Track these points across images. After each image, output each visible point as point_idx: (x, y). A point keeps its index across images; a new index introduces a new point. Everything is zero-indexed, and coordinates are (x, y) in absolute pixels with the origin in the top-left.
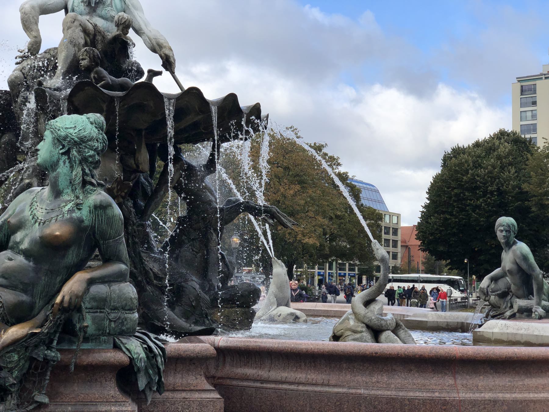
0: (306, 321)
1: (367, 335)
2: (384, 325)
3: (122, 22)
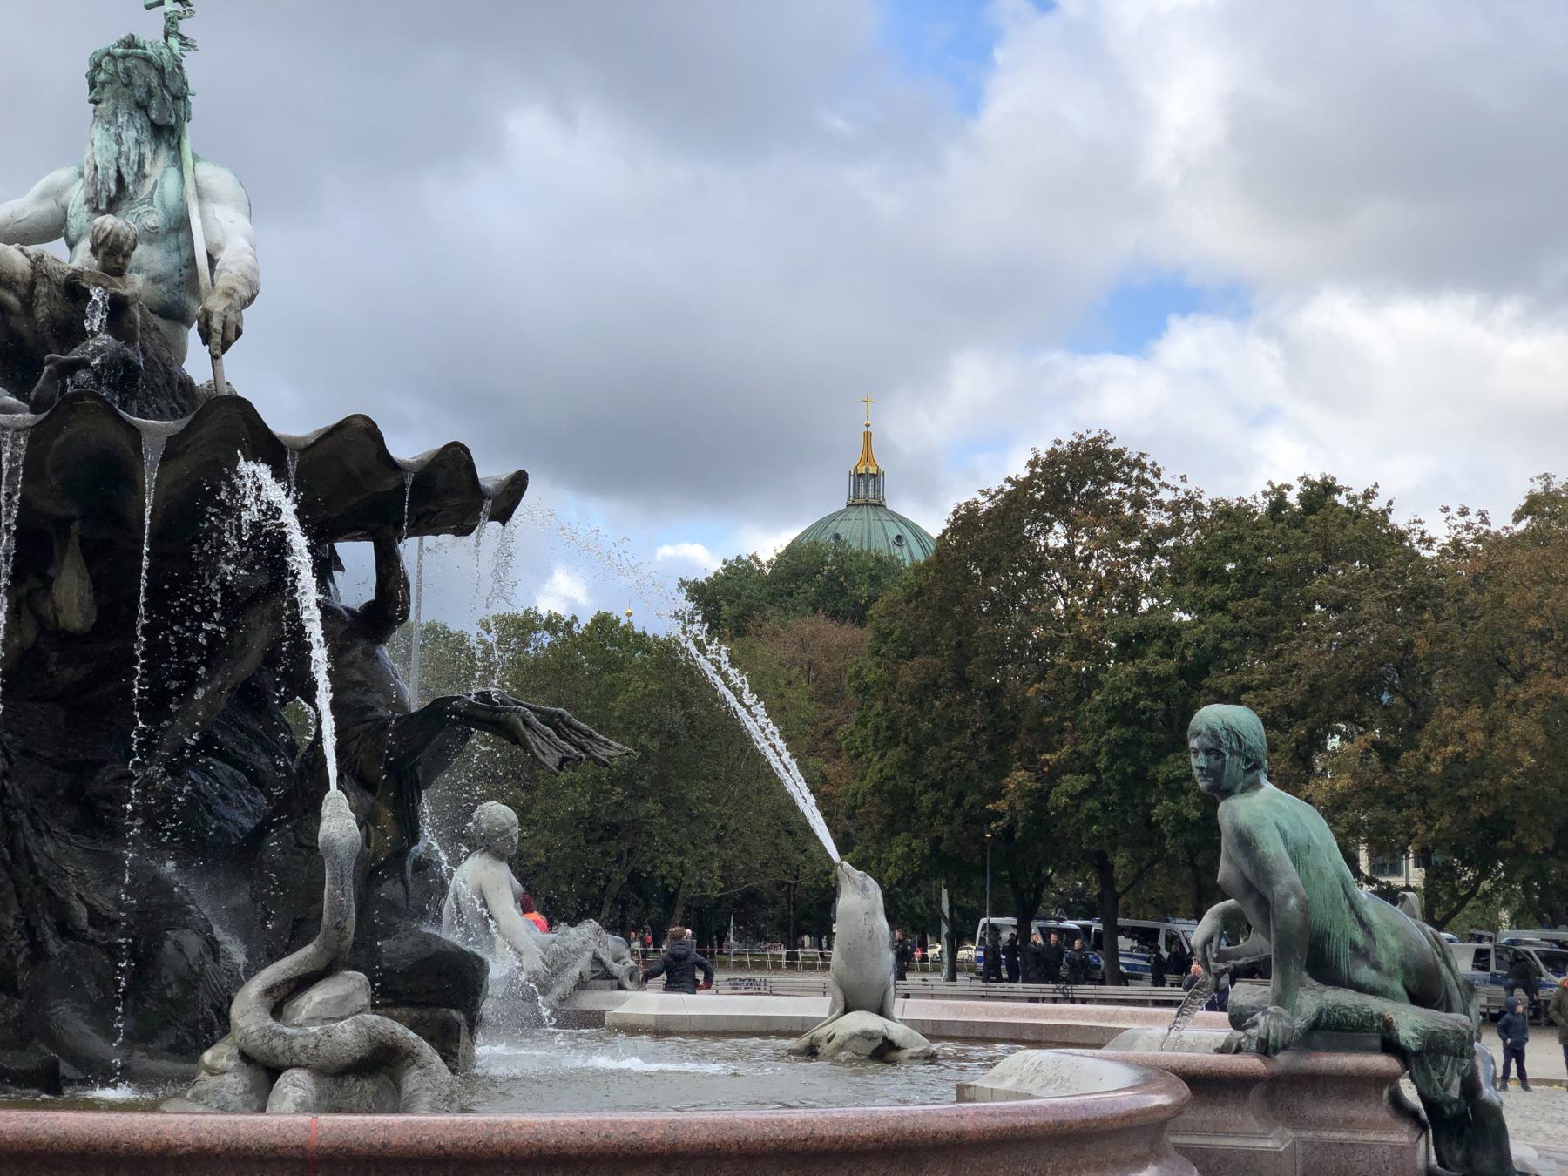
0: (931, 1058)
2: (280, 1049)
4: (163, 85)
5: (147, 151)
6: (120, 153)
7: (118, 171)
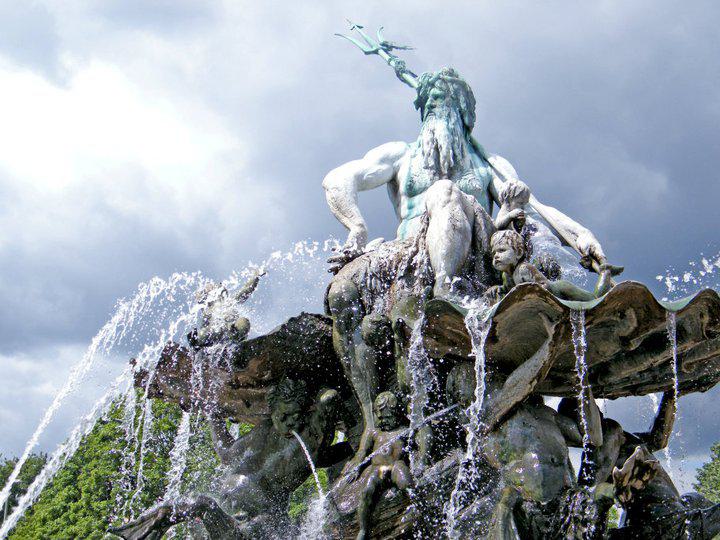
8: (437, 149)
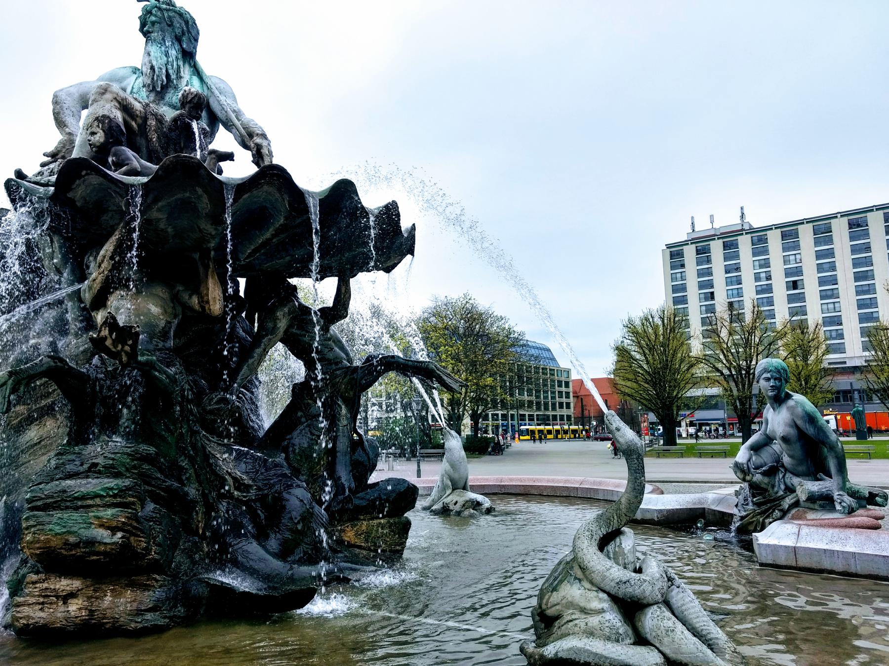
1: (613, 618)
3: (189, 99)
4: (189, 32)
5: (181, 63)
6: (168, 62)
7: (167, 71)
8: (152, 68)
